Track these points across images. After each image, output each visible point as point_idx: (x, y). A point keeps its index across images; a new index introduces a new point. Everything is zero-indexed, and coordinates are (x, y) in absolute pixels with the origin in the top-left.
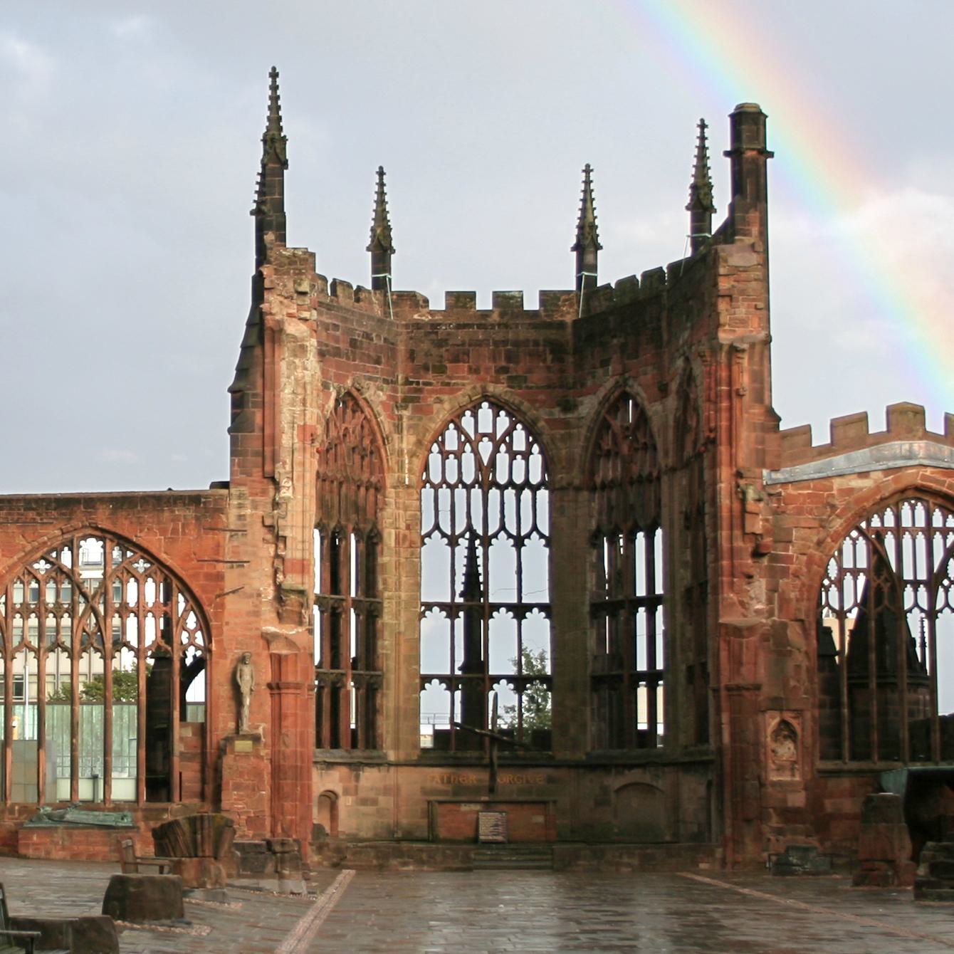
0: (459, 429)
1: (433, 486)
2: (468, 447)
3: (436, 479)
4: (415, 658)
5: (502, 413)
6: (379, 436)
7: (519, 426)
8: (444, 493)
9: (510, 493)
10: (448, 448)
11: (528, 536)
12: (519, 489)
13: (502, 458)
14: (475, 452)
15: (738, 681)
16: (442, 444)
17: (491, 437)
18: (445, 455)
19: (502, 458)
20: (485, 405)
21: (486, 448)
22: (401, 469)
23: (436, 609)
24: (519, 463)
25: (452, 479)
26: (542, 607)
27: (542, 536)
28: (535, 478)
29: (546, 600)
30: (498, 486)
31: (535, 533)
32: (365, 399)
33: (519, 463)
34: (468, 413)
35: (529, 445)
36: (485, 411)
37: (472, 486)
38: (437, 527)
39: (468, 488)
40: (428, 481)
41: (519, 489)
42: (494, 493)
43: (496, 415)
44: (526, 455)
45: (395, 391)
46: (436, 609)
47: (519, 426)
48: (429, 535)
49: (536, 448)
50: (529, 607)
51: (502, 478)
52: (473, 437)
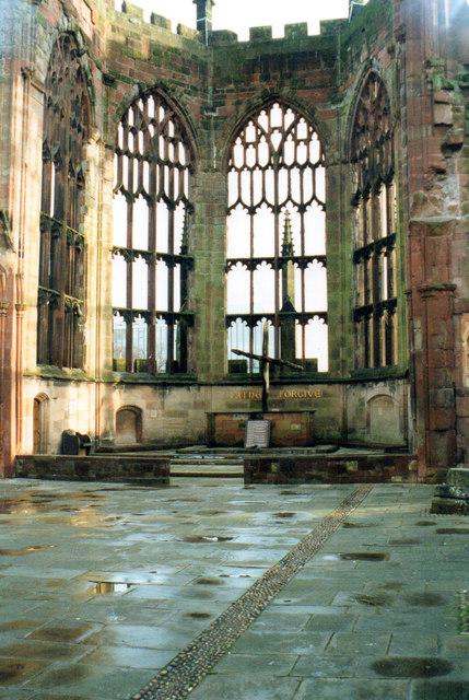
0: (257, 127)
1: (236, 170)
2: (263, 139)
3: (239, 164)
4: (221, 304)
5: (289, 111)
6: (188, 130)
7: (302, 120)
8: (246, 174)
9: (295, 171)
10: (248, 140)
11: (309, 203)
12: (302, 168)
13: (289, 145)
14: (268, 141)
15: (431, 282)
16: (243, 138)
17: (281, 129)
18: (246, 145)
19: (289, 145)
20: (276, 106)
21: (276, 138)
22: (209, 158)
23: (239, 264)
24: (302, 148)
25: (251, 163)
26: (320, 259)
27: (320, 203)
28: (314, 159)
29: (322, 252)
30: (286, 167)
31: (314, 201)
32: (173, 99)
33: (302, 148)
34: (263, 113)
35: (310, 134)
36: (276, 110)
37: (266, 168)
38: (239, 200)
39: (263, 169)
40: (233, 166)
41: (302, 168)
42: (283, 172)
43: (284, 112)
44: (307, 141)
45: (206, 97)
46: (239, 264)
47: (302, 120)
48: (234, 207)
49: (315, 136)
50: (310, 259)
51: (289, 161)
52: (267, 131)
